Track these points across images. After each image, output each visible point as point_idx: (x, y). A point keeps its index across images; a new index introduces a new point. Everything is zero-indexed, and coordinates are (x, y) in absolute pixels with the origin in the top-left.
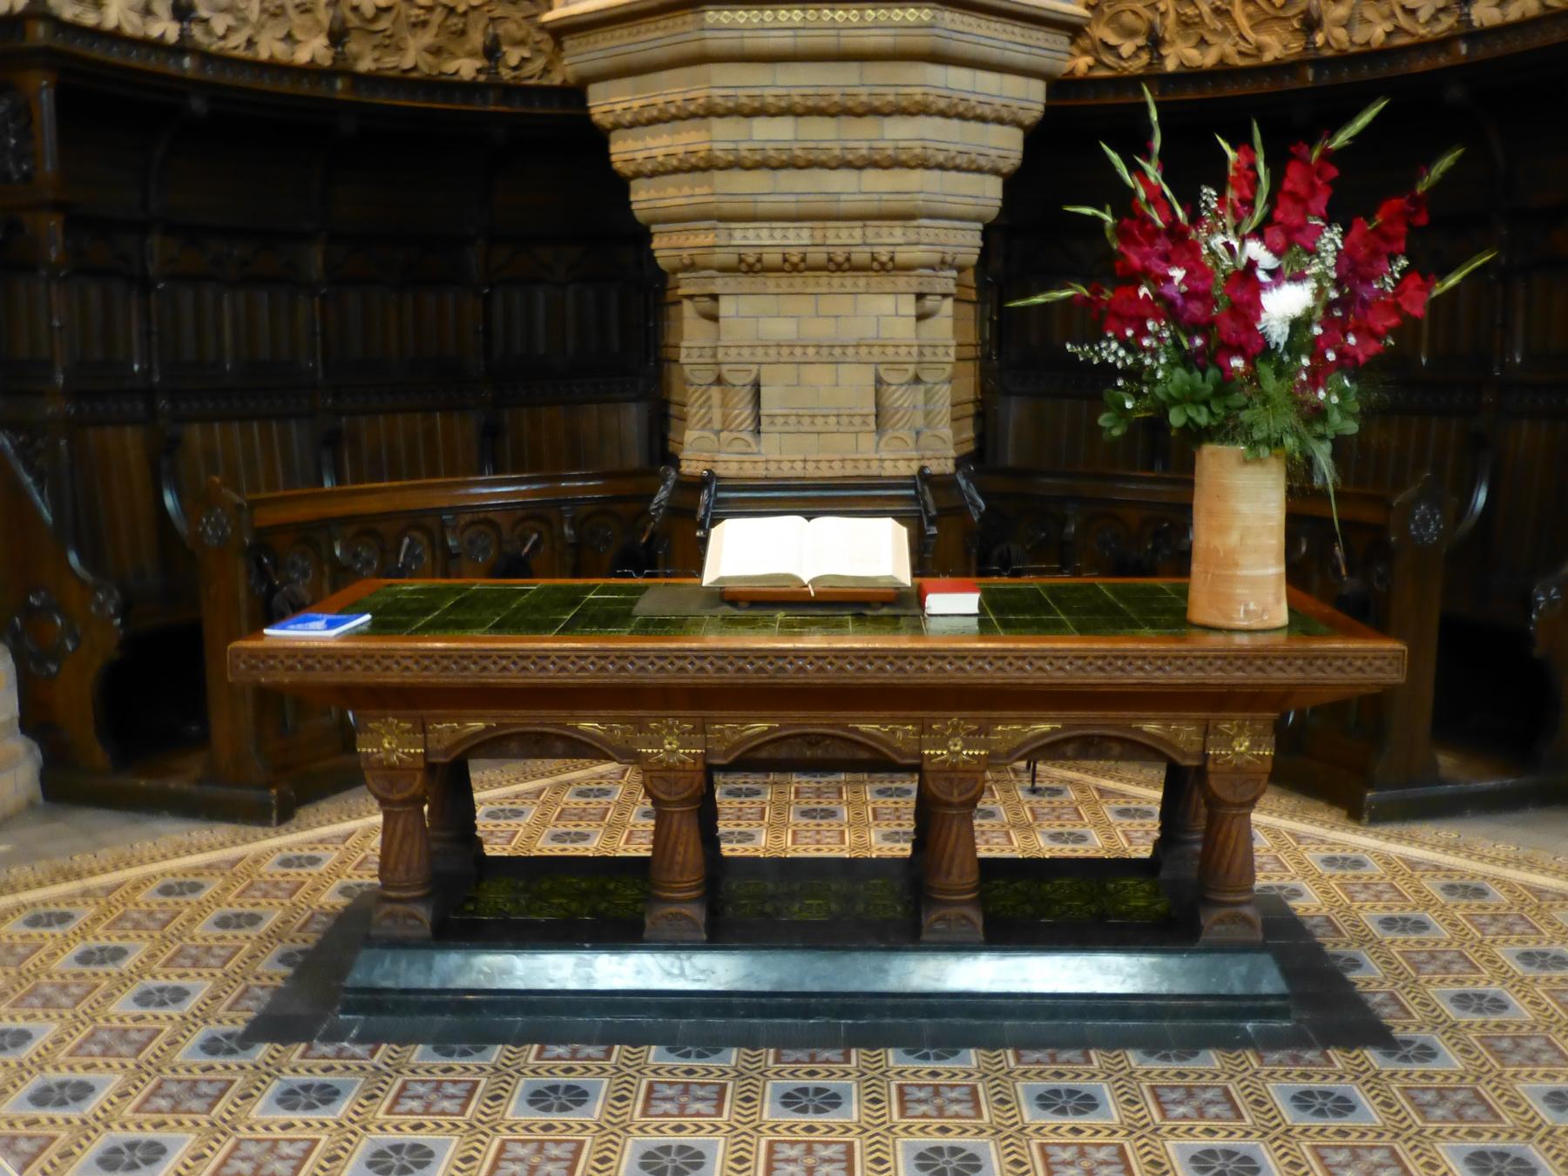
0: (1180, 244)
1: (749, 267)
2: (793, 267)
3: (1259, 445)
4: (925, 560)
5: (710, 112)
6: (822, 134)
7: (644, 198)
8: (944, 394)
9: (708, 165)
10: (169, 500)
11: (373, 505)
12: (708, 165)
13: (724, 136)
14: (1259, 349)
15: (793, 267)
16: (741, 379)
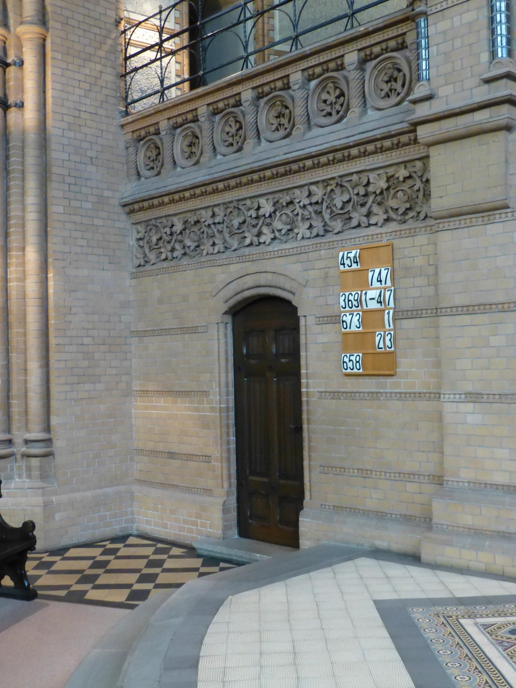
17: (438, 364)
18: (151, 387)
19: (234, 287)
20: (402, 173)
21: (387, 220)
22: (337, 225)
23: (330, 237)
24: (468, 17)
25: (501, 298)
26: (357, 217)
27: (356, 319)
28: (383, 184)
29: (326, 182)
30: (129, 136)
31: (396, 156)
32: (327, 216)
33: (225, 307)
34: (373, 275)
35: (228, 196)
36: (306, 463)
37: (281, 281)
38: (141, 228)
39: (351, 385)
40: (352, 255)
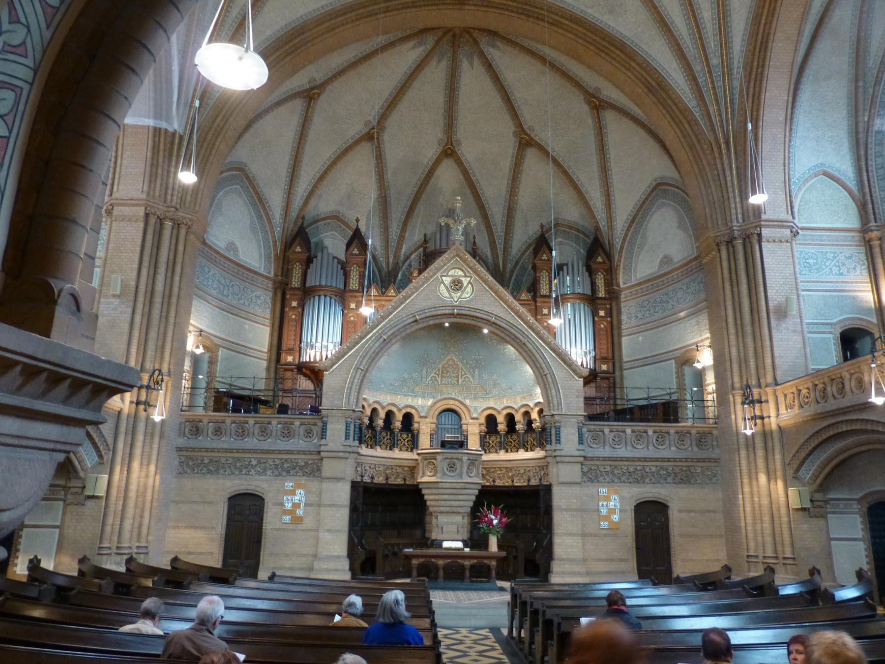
0: (486, 516)
1: (442, 512)
2: (447, 512)
3: (494, 534)
4: (466, 545)
5: (439, 494)
6: (452, 497)
7: (428, 503)
8: (466, 530)
9: (438, 500)
10: (363, 541)
11: (393, 542)
12: (438, 500)
13: (440, 497)
14: (493, 526)
15: (447, 512)
16: (440, 526)
17: (319, 521)
18: (180, 525)
19: (234, 489)
20: (310, 462)
21: (304, 475)
22: (284, 474)
23: (280, 477)
24: (340, 427)
25: (340, 503)
26: (292, 472)
27: (290, 505)
28: (303, 464)
29: (281, 459)
30: (183, 420)
31: (309, 457)
32: (280, 470)
33: (229, 496)
34: (298, 492)
35: (236, 455)
36: (262, 553)
37: (259, 489)
38: (183, 459)
39: (285, 527)
40: (291, 484)
